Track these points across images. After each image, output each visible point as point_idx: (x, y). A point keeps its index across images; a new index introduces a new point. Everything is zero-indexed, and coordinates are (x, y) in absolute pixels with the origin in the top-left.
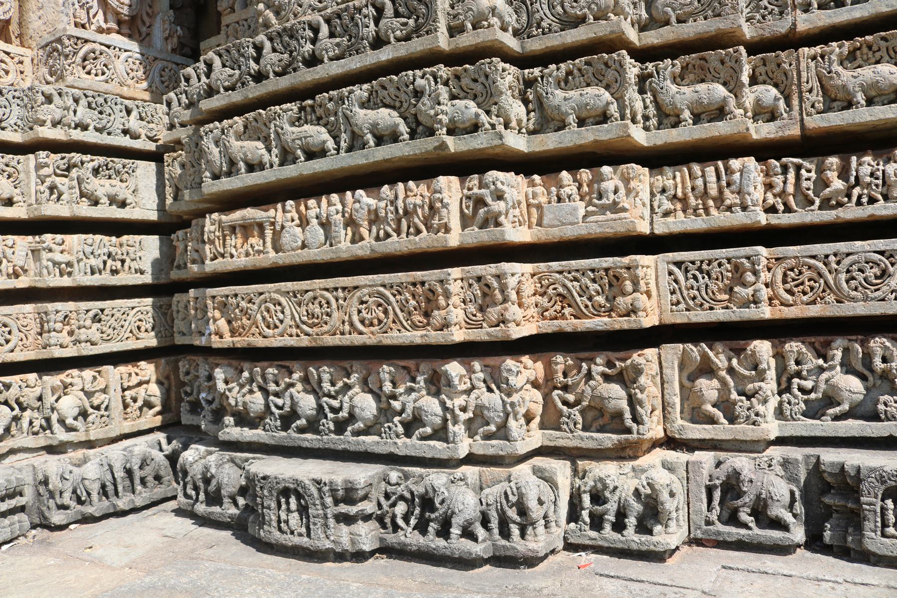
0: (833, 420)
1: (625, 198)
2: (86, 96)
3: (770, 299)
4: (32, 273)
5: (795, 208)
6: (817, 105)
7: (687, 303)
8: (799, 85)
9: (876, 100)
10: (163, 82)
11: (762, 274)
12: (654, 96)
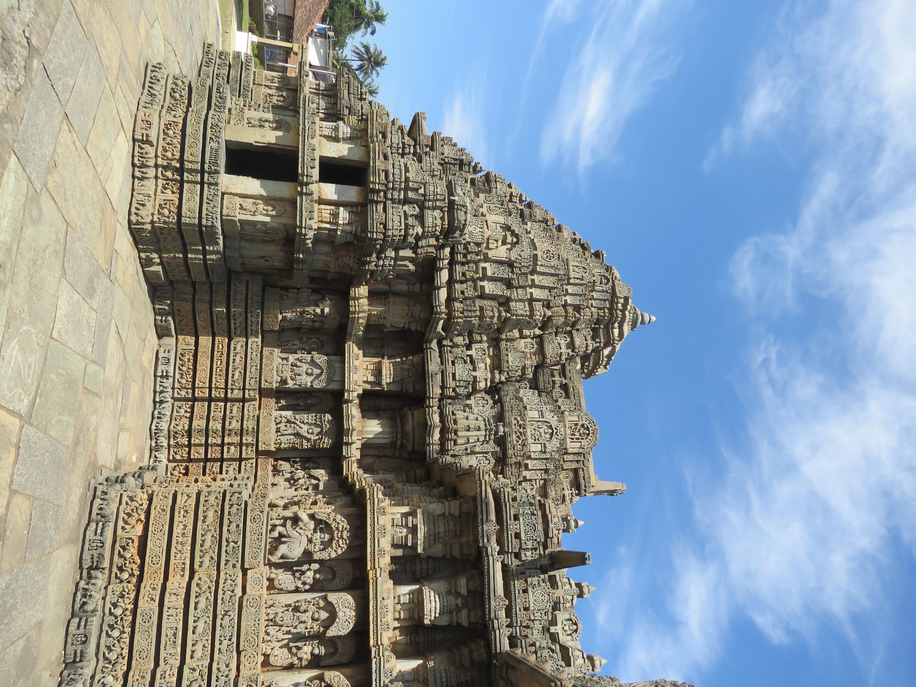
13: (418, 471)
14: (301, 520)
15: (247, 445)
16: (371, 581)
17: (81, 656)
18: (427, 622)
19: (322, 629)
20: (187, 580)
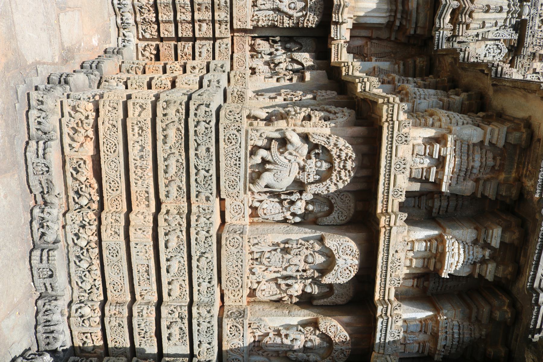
2: (212, 326)
4: (142, 301)
10: (233, 360)
13: (418, 60)
14: (290, 143)
15: (220, 22)
16: (383, 230)
17: (52, 287)
18: (445, 275)
19: (317, 274)
20: (153, 210)
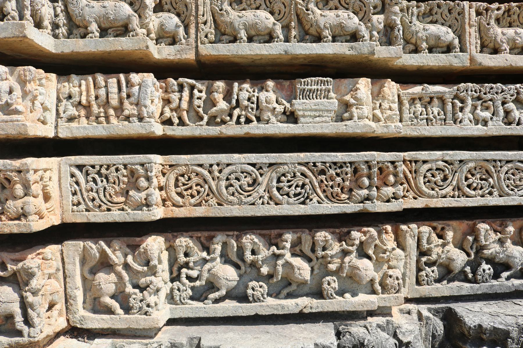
0: (213, 303)
1: (20, 100)
3: (164, 200)
5: (188, 122)
6: (209, 36)
7: (86, 204)
8: (197, 17)
9: (255, 38)
11: (155, 180)
12: (66, 6)
